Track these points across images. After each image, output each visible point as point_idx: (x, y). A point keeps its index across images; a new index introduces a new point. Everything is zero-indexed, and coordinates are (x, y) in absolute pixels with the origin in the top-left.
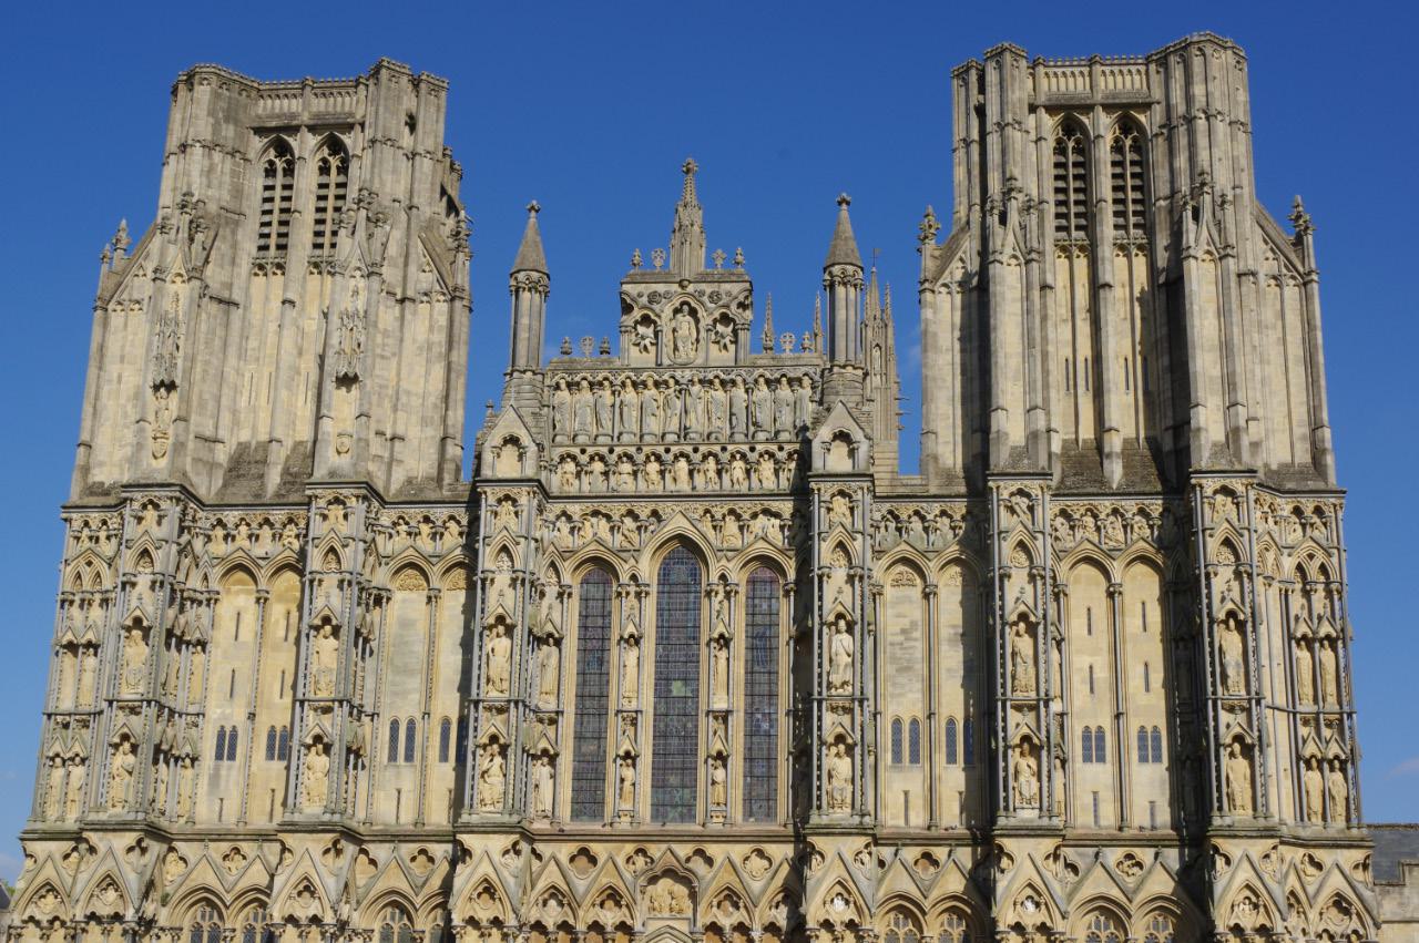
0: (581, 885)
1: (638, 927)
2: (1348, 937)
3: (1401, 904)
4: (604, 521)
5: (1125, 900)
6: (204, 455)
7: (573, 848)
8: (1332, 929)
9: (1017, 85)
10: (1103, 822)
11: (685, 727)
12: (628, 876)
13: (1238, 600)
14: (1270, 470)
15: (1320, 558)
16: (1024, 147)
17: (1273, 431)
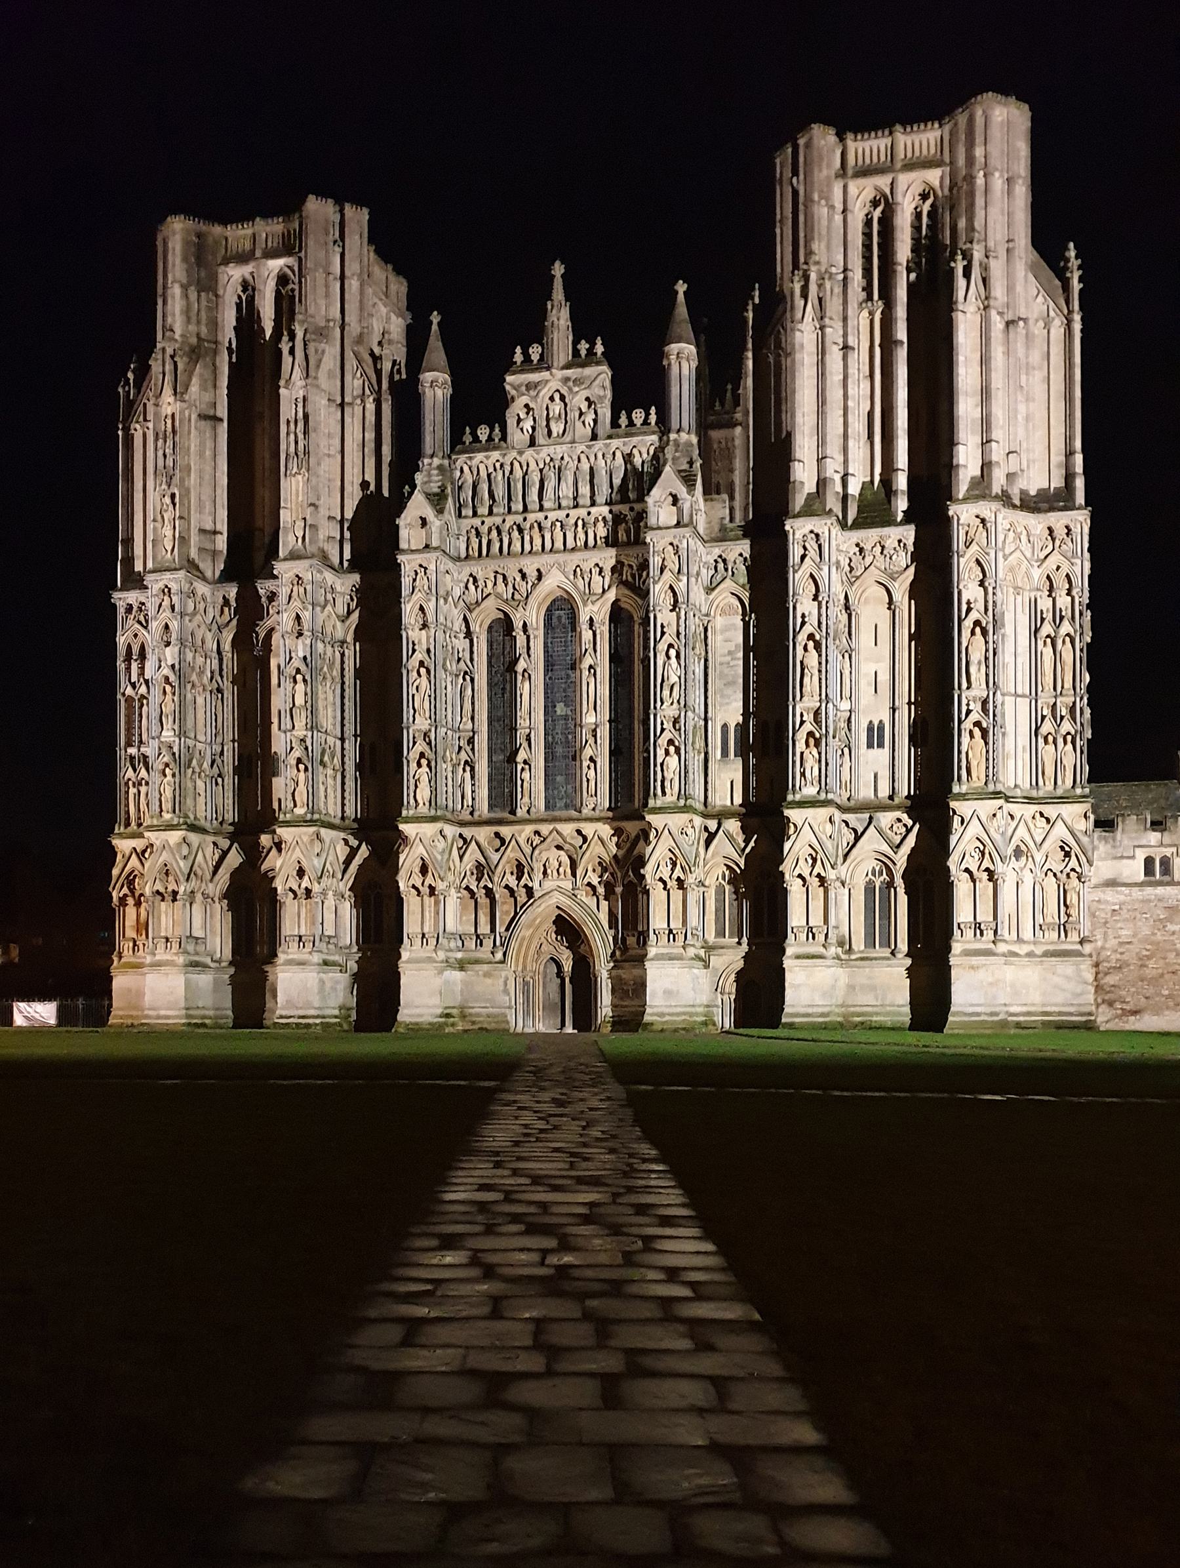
0: (495, 857)
1: (536, 886)
2: (1068, 875)
3: (1114, 847)
4: (500, 578)
5: (892, 853)
6: (209, 546)
7: (489, 831)
8: (1057, 868)
9: (824, 164)
10: (880, 795)
11: (567, 738)
12: (528, 850)
13: (982, 610)
14: (1028, 495)
15: (1065, 569)
16: (830, 219)
17: (1034, 461)
